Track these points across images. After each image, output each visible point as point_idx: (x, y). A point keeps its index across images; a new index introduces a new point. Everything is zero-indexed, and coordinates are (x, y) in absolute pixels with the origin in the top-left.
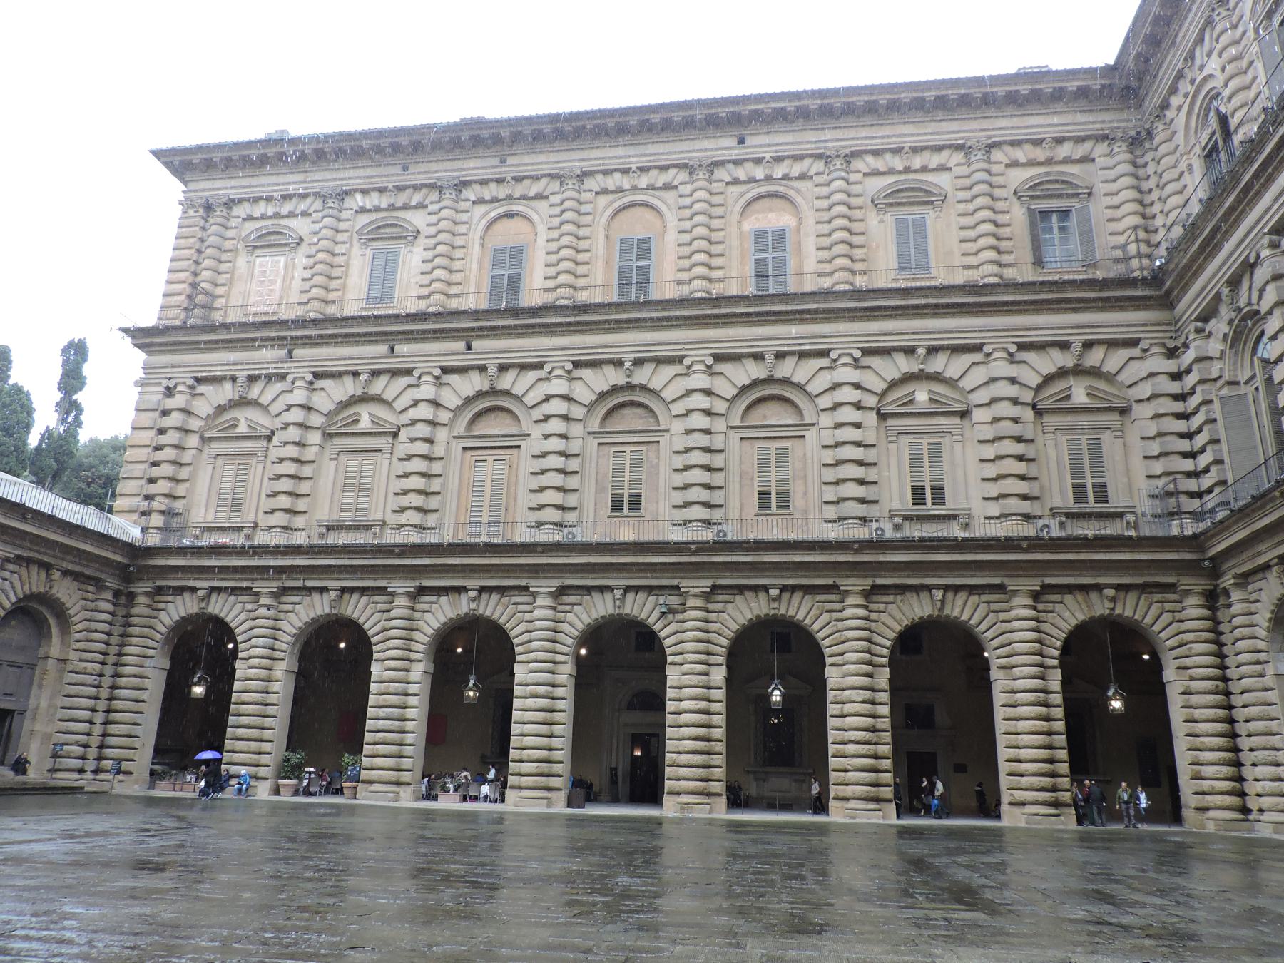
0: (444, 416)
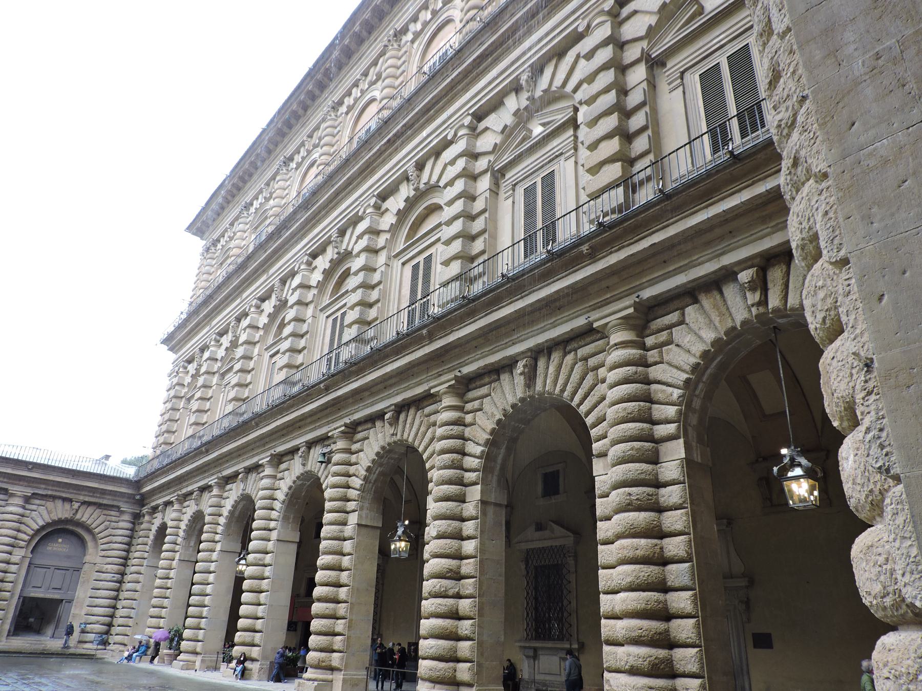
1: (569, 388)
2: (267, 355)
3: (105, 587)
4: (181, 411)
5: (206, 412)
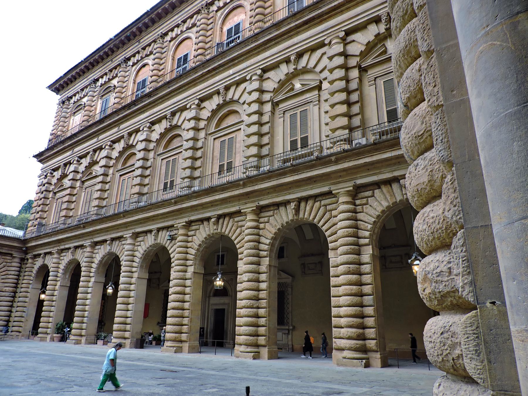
0: (112, 163)
1: (317, 218)
2: (118, 175)
3: (5, 300)
4: (50, 199)
5: (73, 202)
